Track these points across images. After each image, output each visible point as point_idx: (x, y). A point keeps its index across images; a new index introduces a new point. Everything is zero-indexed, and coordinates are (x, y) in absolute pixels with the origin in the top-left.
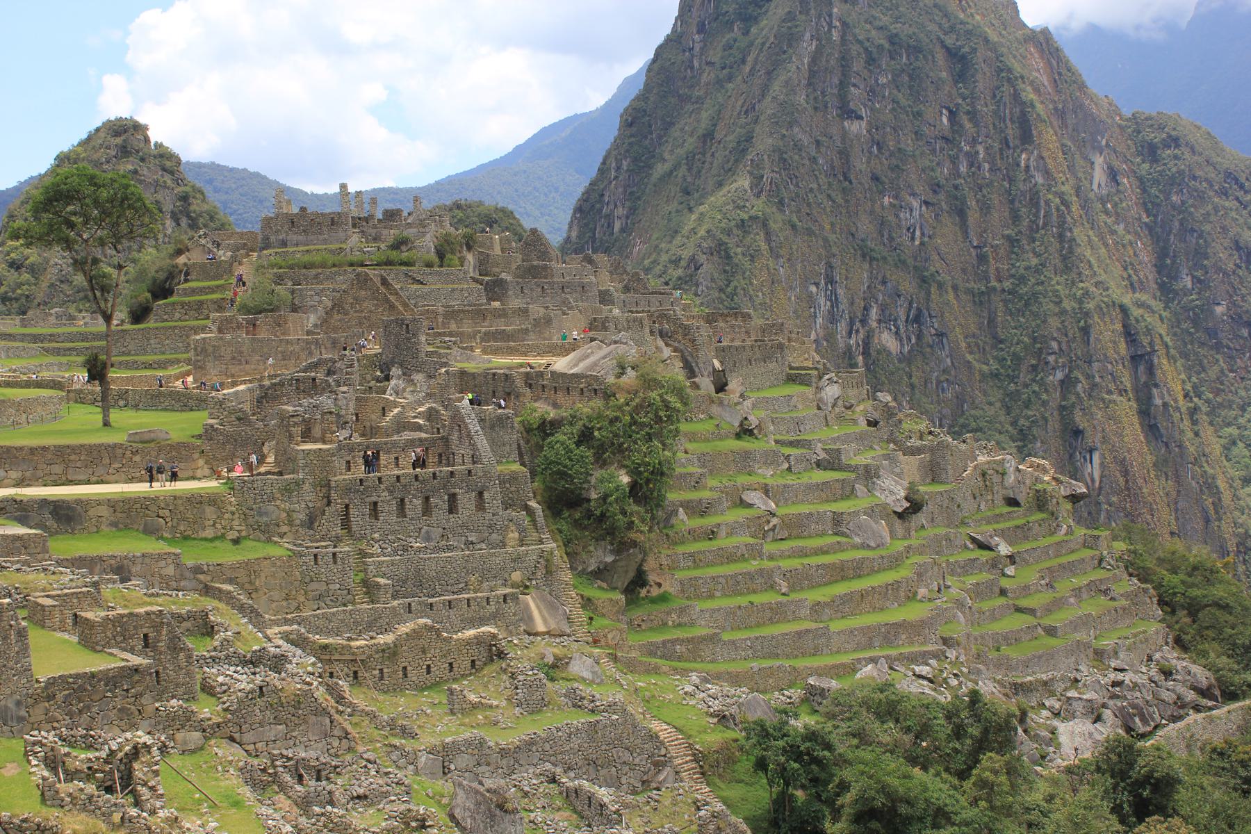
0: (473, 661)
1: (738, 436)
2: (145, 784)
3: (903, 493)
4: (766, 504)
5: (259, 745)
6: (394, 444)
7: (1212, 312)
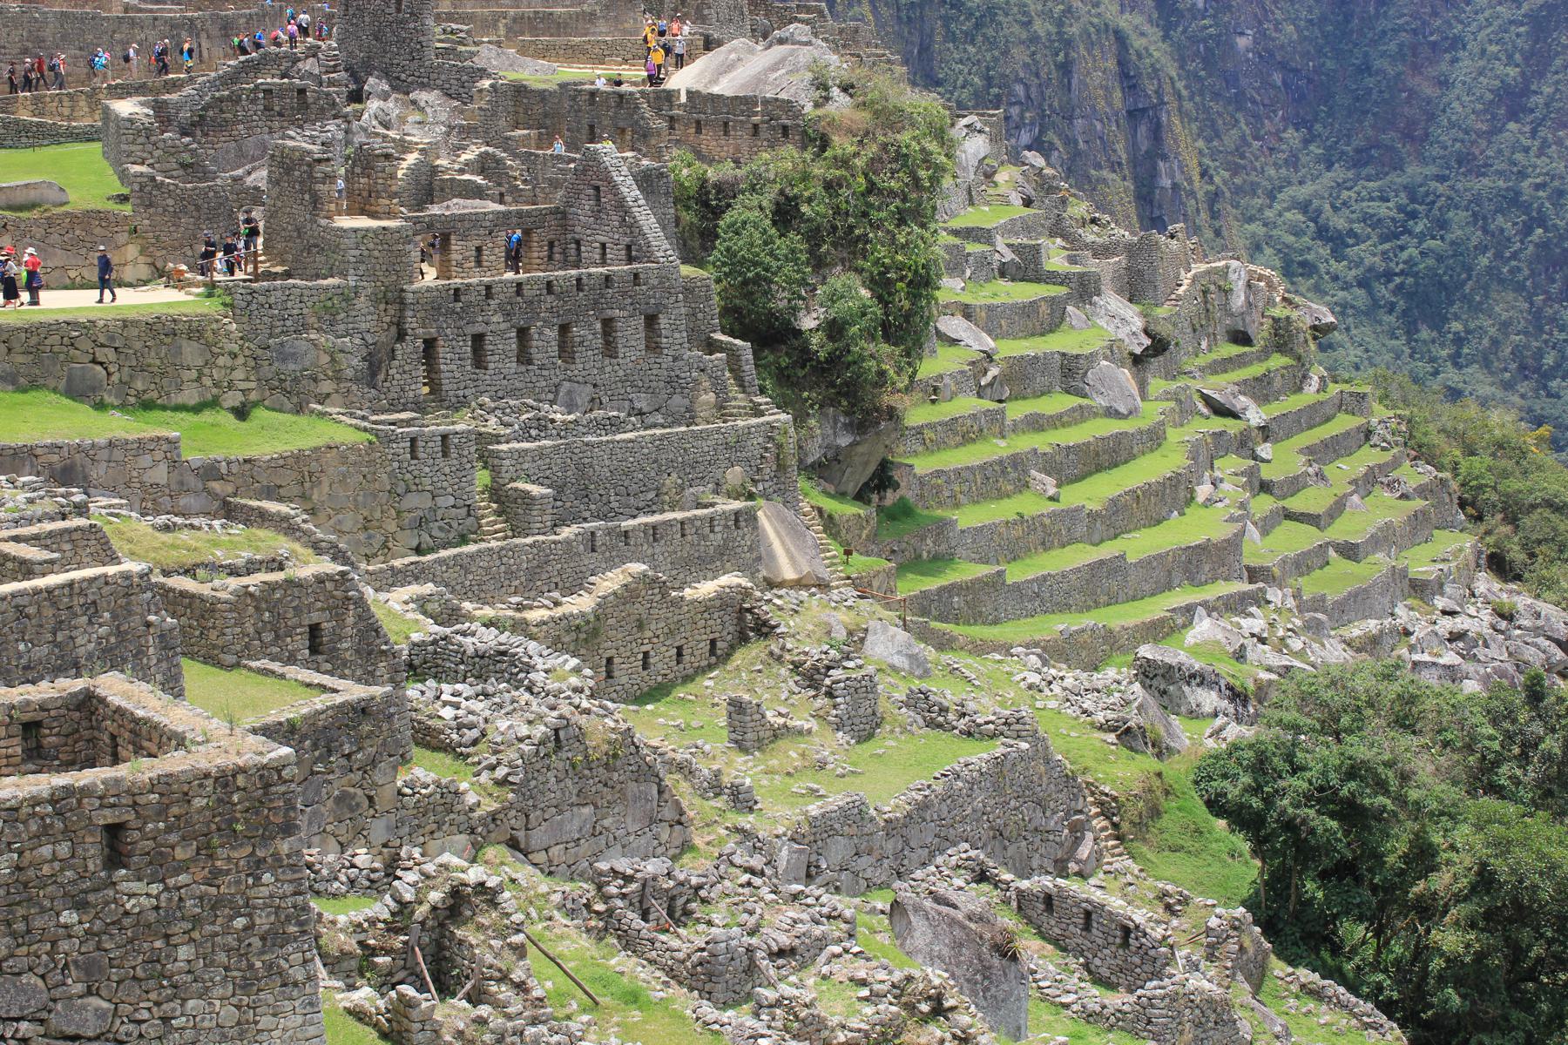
0: (713, 642)
2: (504, 978)
4: (978, 339)
5: (555, 851)
7: (1232, 46)
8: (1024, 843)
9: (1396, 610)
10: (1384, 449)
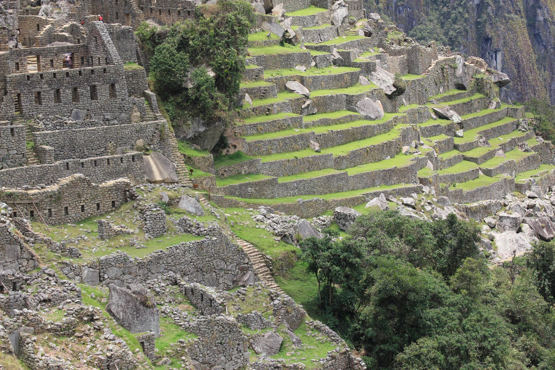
0: (113, 202)
1: (282, 44)
3: (391, 82)
4: (303, 90)
6: (50, 51)
8: (214, 274)
9: (507, 196)
10: (523, 131)
